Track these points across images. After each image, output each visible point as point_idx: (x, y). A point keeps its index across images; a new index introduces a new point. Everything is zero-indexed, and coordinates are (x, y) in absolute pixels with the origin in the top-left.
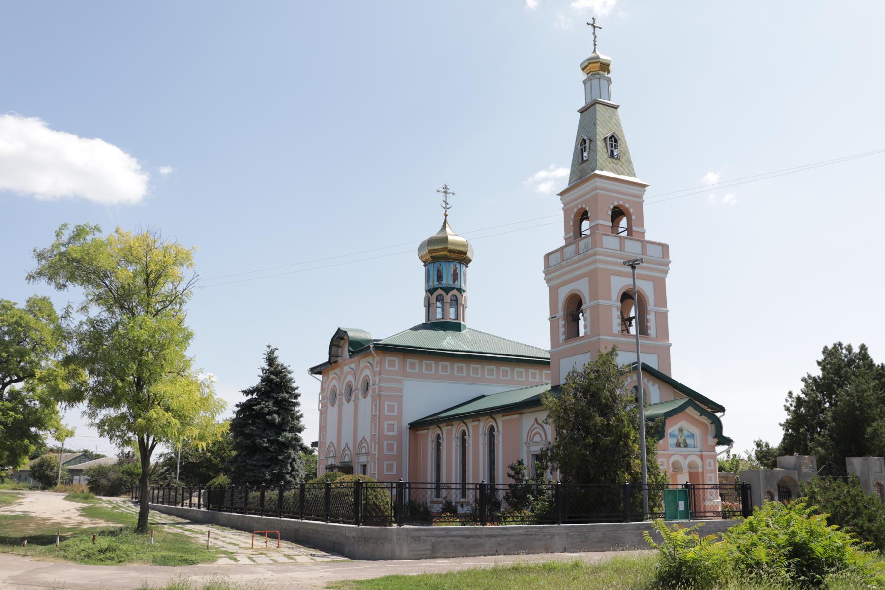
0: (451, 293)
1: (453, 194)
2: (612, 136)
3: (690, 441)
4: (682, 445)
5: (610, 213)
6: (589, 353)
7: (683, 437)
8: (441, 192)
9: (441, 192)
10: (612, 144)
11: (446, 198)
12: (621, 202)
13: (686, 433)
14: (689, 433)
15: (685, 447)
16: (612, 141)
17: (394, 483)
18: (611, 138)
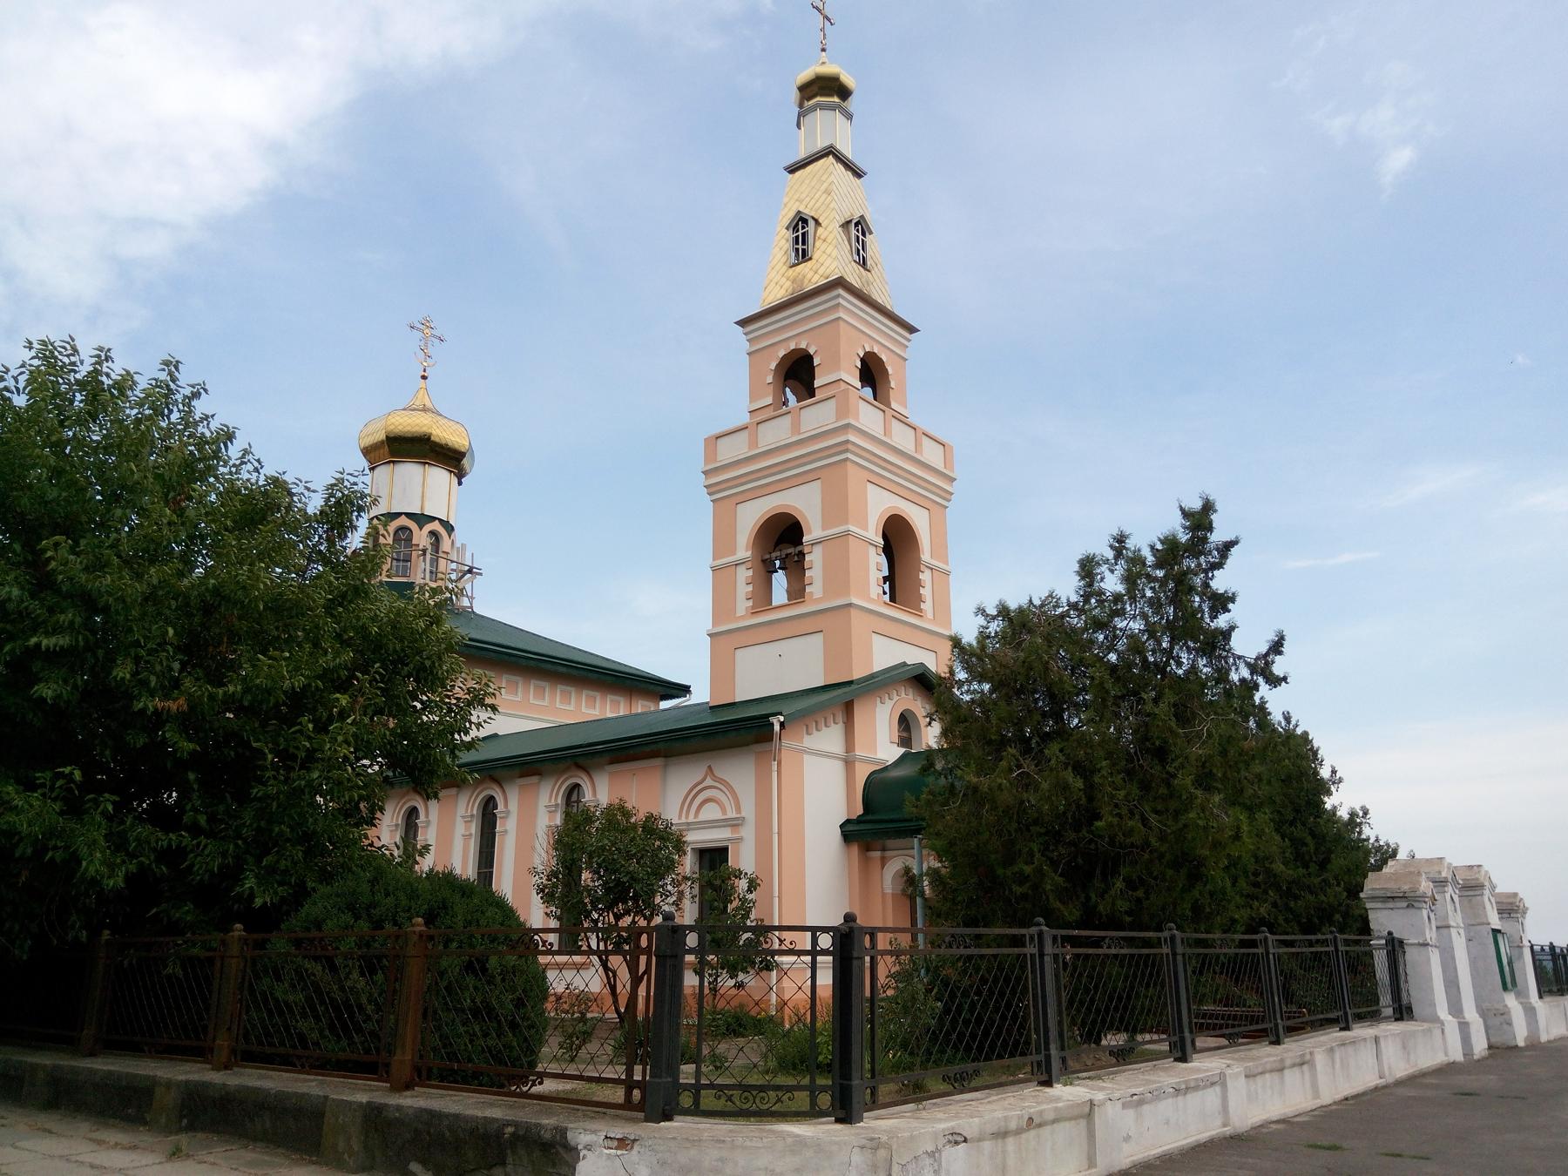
6: (819, 638)
17: (825, 930)
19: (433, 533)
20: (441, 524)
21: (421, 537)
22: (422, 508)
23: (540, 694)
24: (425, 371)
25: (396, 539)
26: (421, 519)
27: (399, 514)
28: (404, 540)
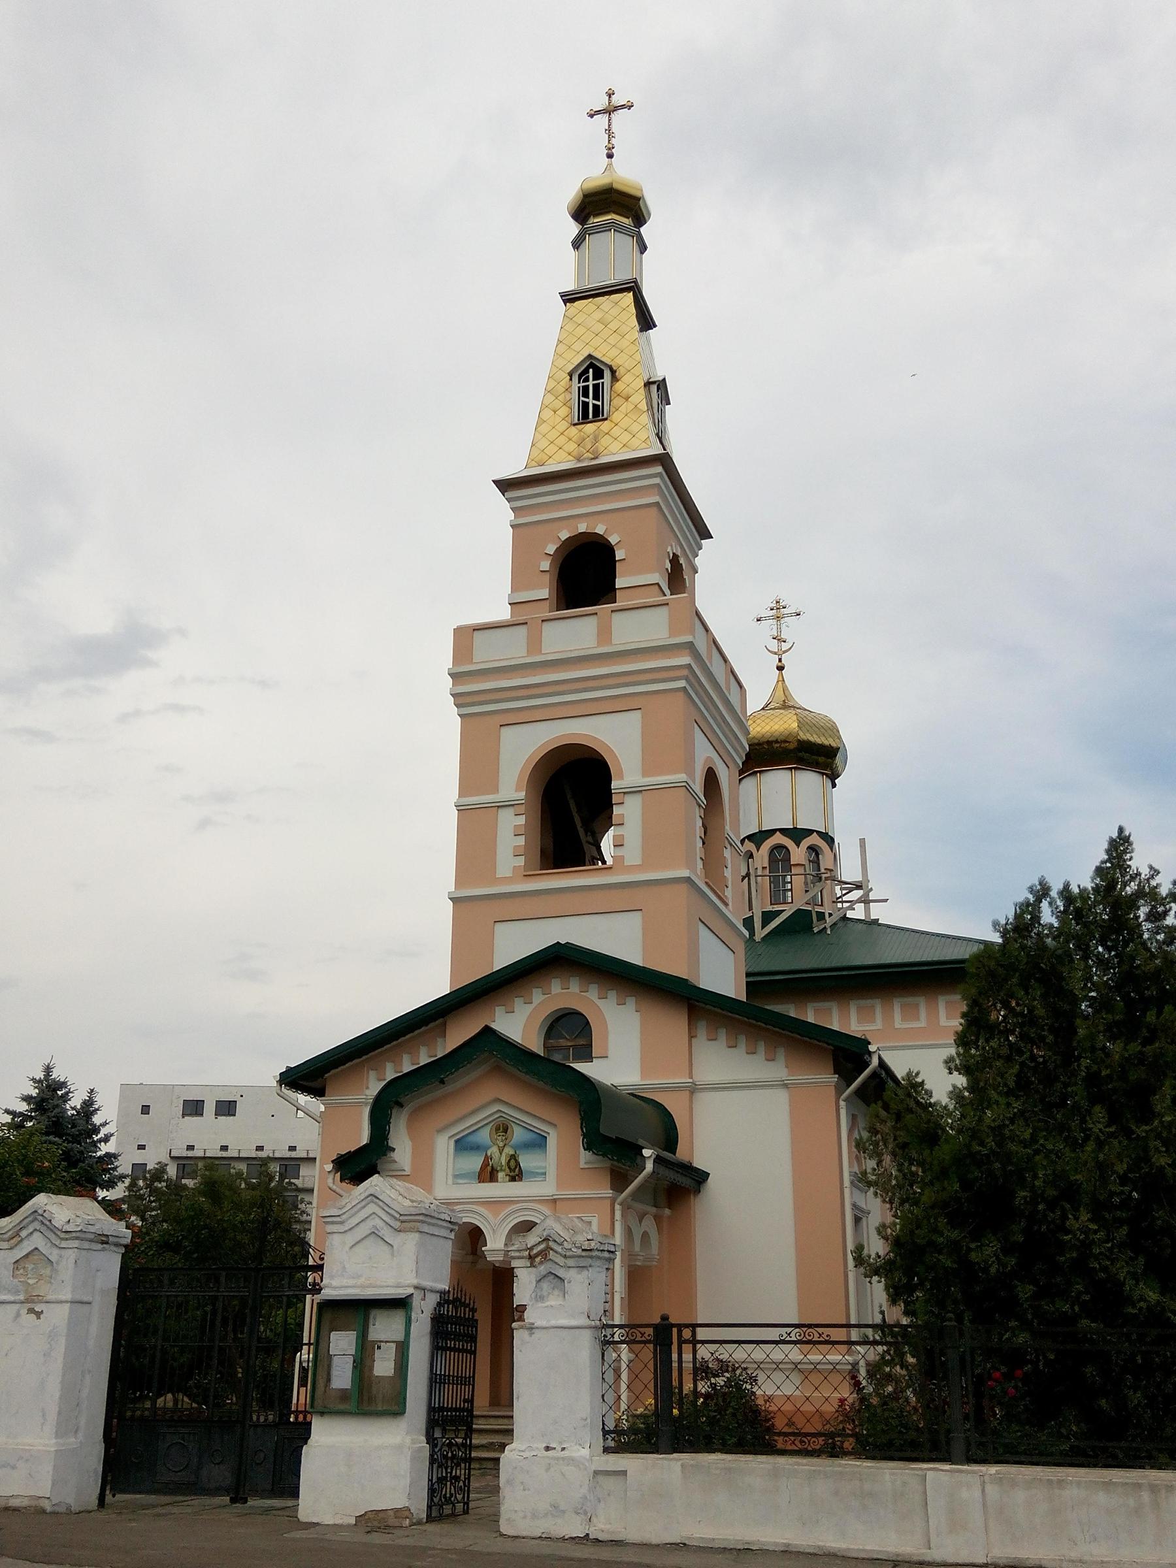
0: (806, 843)
1: (778, 611)
2: (592, 365)
3: (527, 1161)
4: (501, 1175)
5: (546, 565)
7: (509, 1151)
8: (766, 618)
9: (766, 618)
10: (586, 389)
11: (779, 630)
12: (582, 528)
13: (518, 1134)
14: (529, 1136)
15: (513, 1179)
16: (587, 380)
18: (586, 371)
19: (813, 849)
20: (781, 833)
21: (798, 854)
22: (760, 824)
23: (910, 1013)
24: (780, 660)
25: (773, 860)
26: (797, 834)
27: (773, 832)
28: (781, 860)
